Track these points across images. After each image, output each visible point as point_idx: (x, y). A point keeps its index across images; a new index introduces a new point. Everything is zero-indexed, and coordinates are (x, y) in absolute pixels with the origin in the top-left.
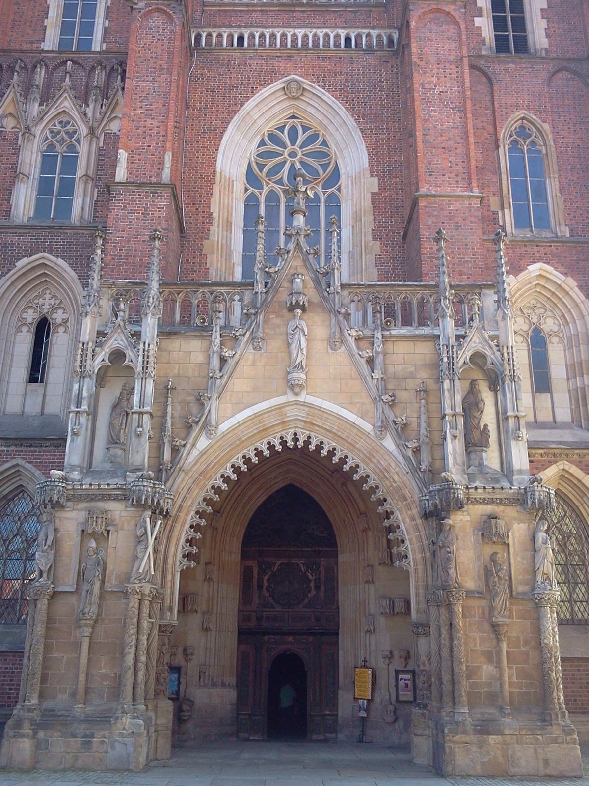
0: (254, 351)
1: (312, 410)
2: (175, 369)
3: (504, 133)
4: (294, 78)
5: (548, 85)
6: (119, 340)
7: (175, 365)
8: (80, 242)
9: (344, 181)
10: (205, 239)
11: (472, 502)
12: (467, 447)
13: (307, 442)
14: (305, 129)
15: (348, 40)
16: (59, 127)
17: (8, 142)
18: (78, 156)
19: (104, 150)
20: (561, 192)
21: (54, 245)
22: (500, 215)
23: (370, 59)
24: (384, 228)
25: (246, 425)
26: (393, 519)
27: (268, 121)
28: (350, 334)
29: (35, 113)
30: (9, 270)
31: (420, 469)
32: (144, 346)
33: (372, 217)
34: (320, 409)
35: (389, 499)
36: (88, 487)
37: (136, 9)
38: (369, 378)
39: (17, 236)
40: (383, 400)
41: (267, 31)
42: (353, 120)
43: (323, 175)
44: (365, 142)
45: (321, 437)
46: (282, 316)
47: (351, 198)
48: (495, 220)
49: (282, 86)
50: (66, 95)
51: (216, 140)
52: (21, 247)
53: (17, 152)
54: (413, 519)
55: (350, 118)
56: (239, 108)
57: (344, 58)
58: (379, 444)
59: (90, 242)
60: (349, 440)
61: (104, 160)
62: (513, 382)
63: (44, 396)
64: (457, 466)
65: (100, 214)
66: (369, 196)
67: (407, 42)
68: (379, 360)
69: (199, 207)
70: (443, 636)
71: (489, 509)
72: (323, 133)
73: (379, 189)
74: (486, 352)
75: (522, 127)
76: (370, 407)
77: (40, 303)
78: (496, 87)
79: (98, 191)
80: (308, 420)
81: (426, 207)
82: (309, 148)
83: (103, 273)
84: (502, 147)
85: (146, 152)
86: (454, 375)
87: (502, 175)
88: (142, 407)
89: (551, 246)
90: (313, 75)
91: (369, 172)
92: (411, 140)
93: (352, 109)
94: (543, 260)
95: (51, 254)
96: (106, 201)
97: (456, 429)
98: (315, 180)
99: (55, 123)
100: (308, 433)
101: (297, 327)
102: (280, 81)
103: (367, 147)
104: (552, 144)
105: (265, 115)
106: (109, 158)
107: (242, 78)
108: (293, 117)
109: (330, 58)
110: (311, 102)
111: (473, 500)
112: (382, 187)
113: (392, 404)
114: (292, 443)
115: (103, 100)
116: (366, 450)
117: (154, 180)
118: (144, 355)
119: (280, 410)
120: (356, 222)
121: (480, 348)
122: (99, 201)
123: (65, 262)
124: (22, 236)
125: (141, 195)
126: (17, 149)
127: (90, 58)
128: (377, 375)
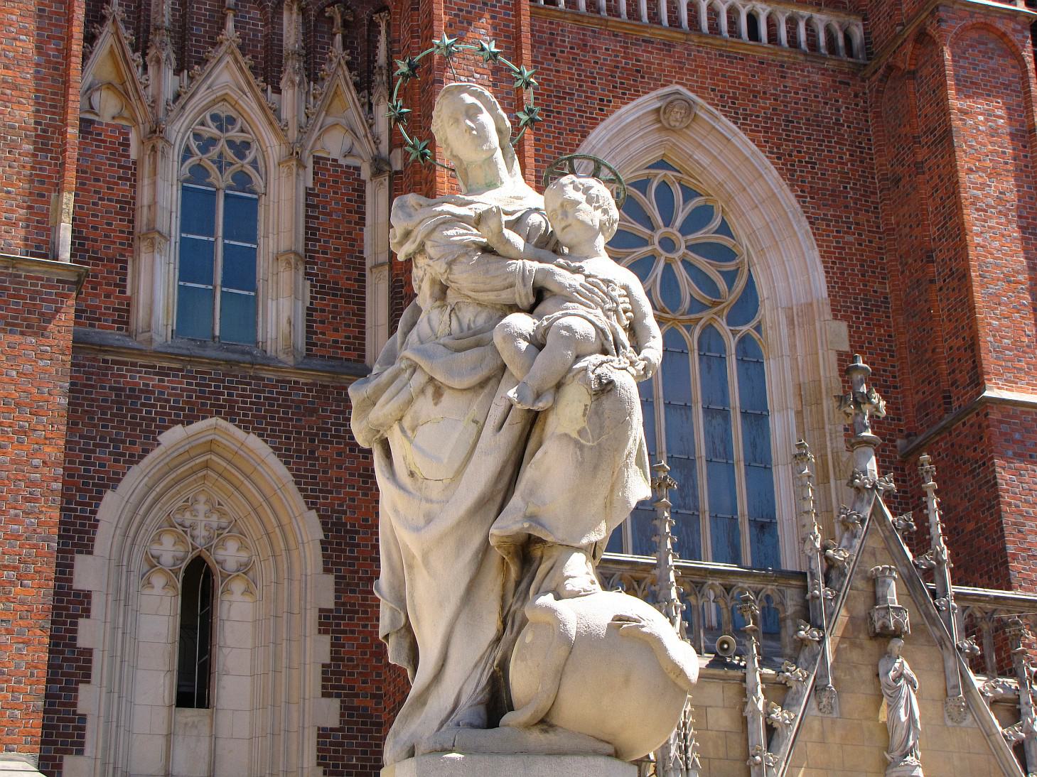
0: (820, 714)
4: (677, 93)
8: (293, 401)
9: (766, 312)
14: (689, 194)
16: (211, 130)
17: (106, 148)
18: (256, 200)
19: (317, 196)
21: (237, 402)
29: (168, 94)
30: (146, 451)
39: (156, 374)
43: (731, 297)
46: (861, 647)
52: (168, 401)
53: (131, 174)
56: (580, 141)
57: (769, 65)
59: (313, 403)
61: (317, 218)
63: (214, 738)
65: (319, 339)
66: (833, 358)
67: (913, 68)
72: (723, 210)
73: (851, 346)
77: (187, 523)
79: (313, 286)
81: (1001, 422)
82: (698, 234)
90: (713, 90)
91: (828, 309)
93: (789, 171)
95: (232, 421)
96: (330, 312)
98: (715, 304)
102: (653, 94)
103: (822, 257)
106: (330, 214)
107: (579, 75)
109: (742, 59)
115: (308, 83)
122: (316, 310)
123: (263, 443)
124: (168, 375)
126: (130, 168)
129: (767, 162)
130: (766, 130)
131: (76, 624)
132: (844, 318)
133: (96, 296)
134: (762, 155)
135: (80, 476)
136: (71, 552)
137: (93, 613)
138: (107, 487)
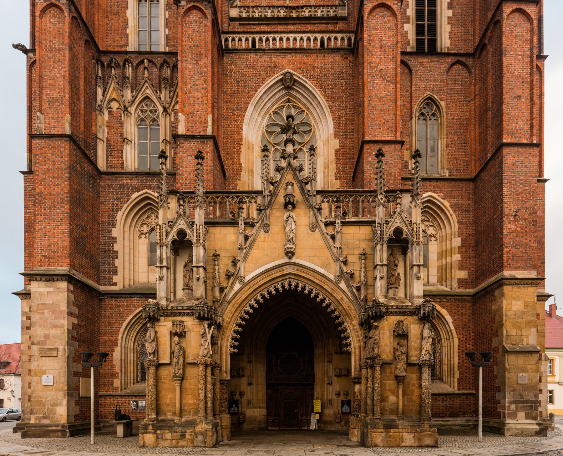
1: (299, 267)
5: (447, 75)
13: (297, 286)
16: (145, 108)
25: (261, 276)
31: (360, 298)
55: (322, 97)
70: (369, 383)
76: (333, 265)
78: (414, 76)
92: (361, 109)
99: (143, 105)
129: (317, 90)
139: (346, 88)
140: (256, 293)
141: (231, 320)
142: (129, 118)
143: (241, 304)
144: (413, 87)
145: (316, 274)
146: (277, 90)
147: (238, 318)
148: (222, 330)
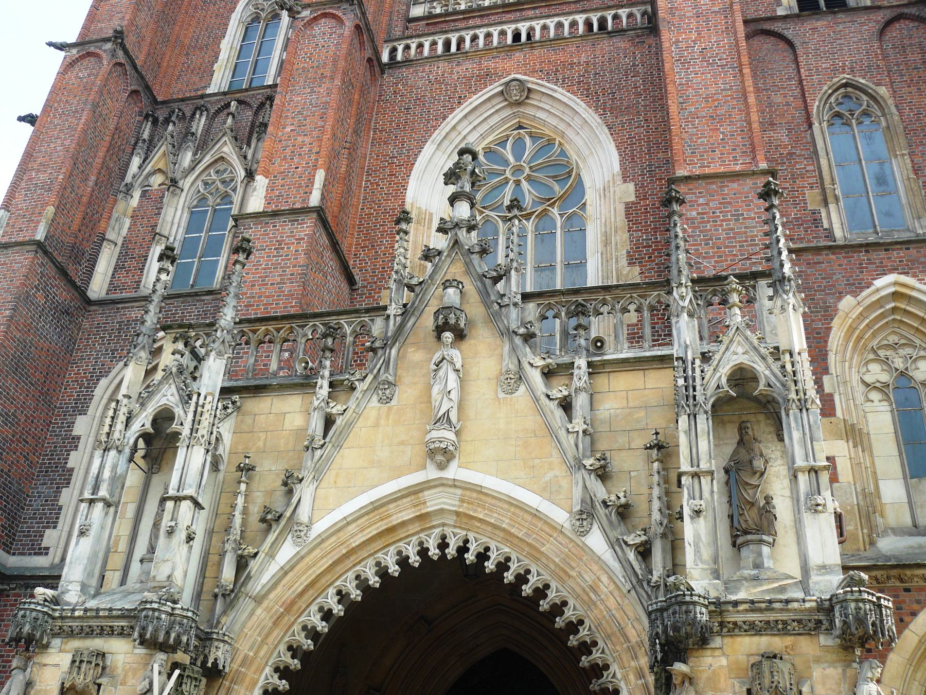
0: (379, 405)
1: (468, 493)
2: (260, 440)
3: (818, 107)
6: (169, 395)
7: (261, 434)
9: (591, 197)
10: (385, 288)
11: (729, 631)
12: (734, 538)
14: (534, 137)
15: (589, 24)
20: (916, 174)
22: (824, 214)
23: (621, 43)
24: (644, 247)
25: (359, 522)
26: (607, 677)
27: (483, 137)
28: (531, 365)
31: (649, 582)
32: (198, 399)
33: (627, 235)
34: (479, 490)
35: (601, 644)
36: (81, 613)
37: (298, 18)
38: (562, 433)
40: (585, 466)
41: (481, 30)
42: (596, 117)
44: (614, 140)
45: (485, 539)
47: (598, 217)
48: (817, 221)
49: (500, 89)
50: (225, 138)
51: (408, 165)
54: (640, 675)
55: (593, 114)
58: (581, 544)
60: (530, 541)
62: (804, 411)
64: (701, 566)
66: (621, 208)
68: (581, 402)
69: (380, 249)
71: (764, 643)
72: (560, 143)
73: (636, 197)
74: (755, 366)
75: (846, 96)
78: (800, 51)
80: (461, 510)
83: (163, 304)
84: (817, 124)
85: (293, 175)
86: (695, 405)
87: (821, 160)
88: (181, 490)
89: (908, 249)
94: (898, 269)
97: (701, 498)
98: (549, 200)
100: (464, 533)
101: (443, 359)
102: (497, 84)
104: (893, 109)
105: (478, 129)
108: (520, 127)
110: (541, 105)
111: (731, 626)
112: (641, 195)
113: (603, 474)
114: (437, 551)
116: (557, 556)
117: (298, 206)
118: (195, 412)
119: (416, 496)
120: (606, 246)
121: (744, 359)
125: (276, 226)
127: (259, 94)
128: (578, 425)
129: (578, 101)
130: (579, 83)
131: (68, 455)
132: (632, 180)
133: (127, 277)
134: (575, 98)
135: (90, 373)
136: (76, 415)
137: (79, 448)
138: (103, 376)
139: (645, 91)
140: (339, 569)
141: (256, 653)
142: (177, 198)
143: (293, 603)
144: (802, 71)
145: (518, 511)
146: (493, 110)
147: (282, 647)
148: (227, 683)
